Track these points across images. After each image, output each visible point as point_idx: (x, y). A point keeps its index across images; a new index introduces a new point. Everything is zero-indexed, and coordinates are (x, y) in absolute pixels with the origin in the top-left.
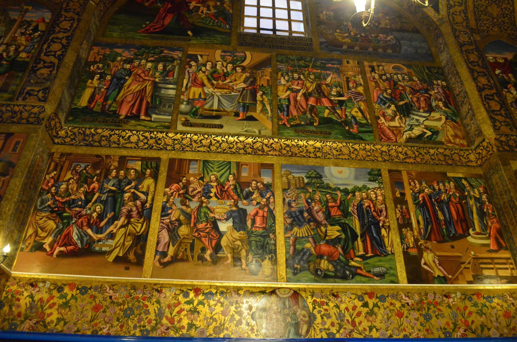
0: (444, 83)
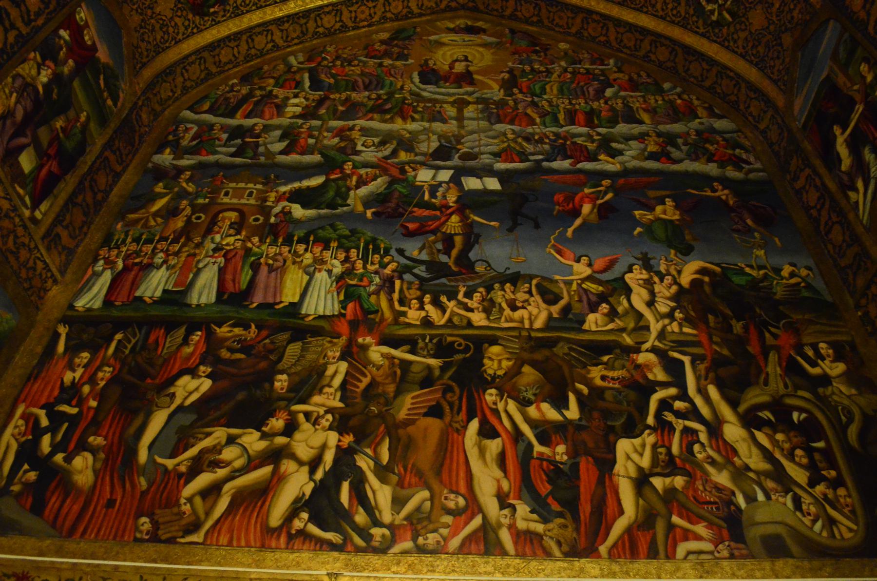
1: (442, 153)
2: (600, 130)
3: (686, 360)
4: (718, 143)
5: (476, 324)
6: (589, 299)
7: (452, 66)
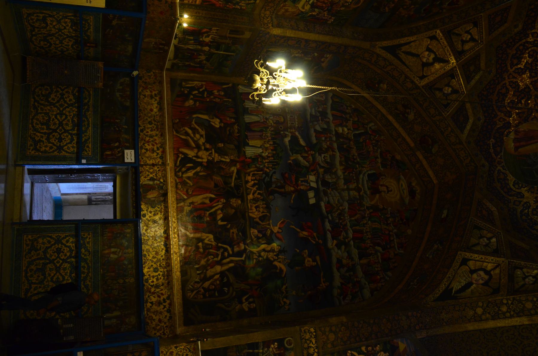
1: (325, 183)
3: (243, 258)
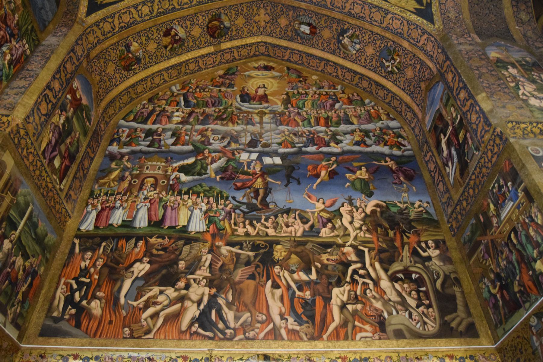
0: (28, 52)
1: (253, 144)
2: (331, 128)
3: (366, 250)
4: (390, 135)
5: (270, 235)
6: (322, 221)
7: (257, 92)
